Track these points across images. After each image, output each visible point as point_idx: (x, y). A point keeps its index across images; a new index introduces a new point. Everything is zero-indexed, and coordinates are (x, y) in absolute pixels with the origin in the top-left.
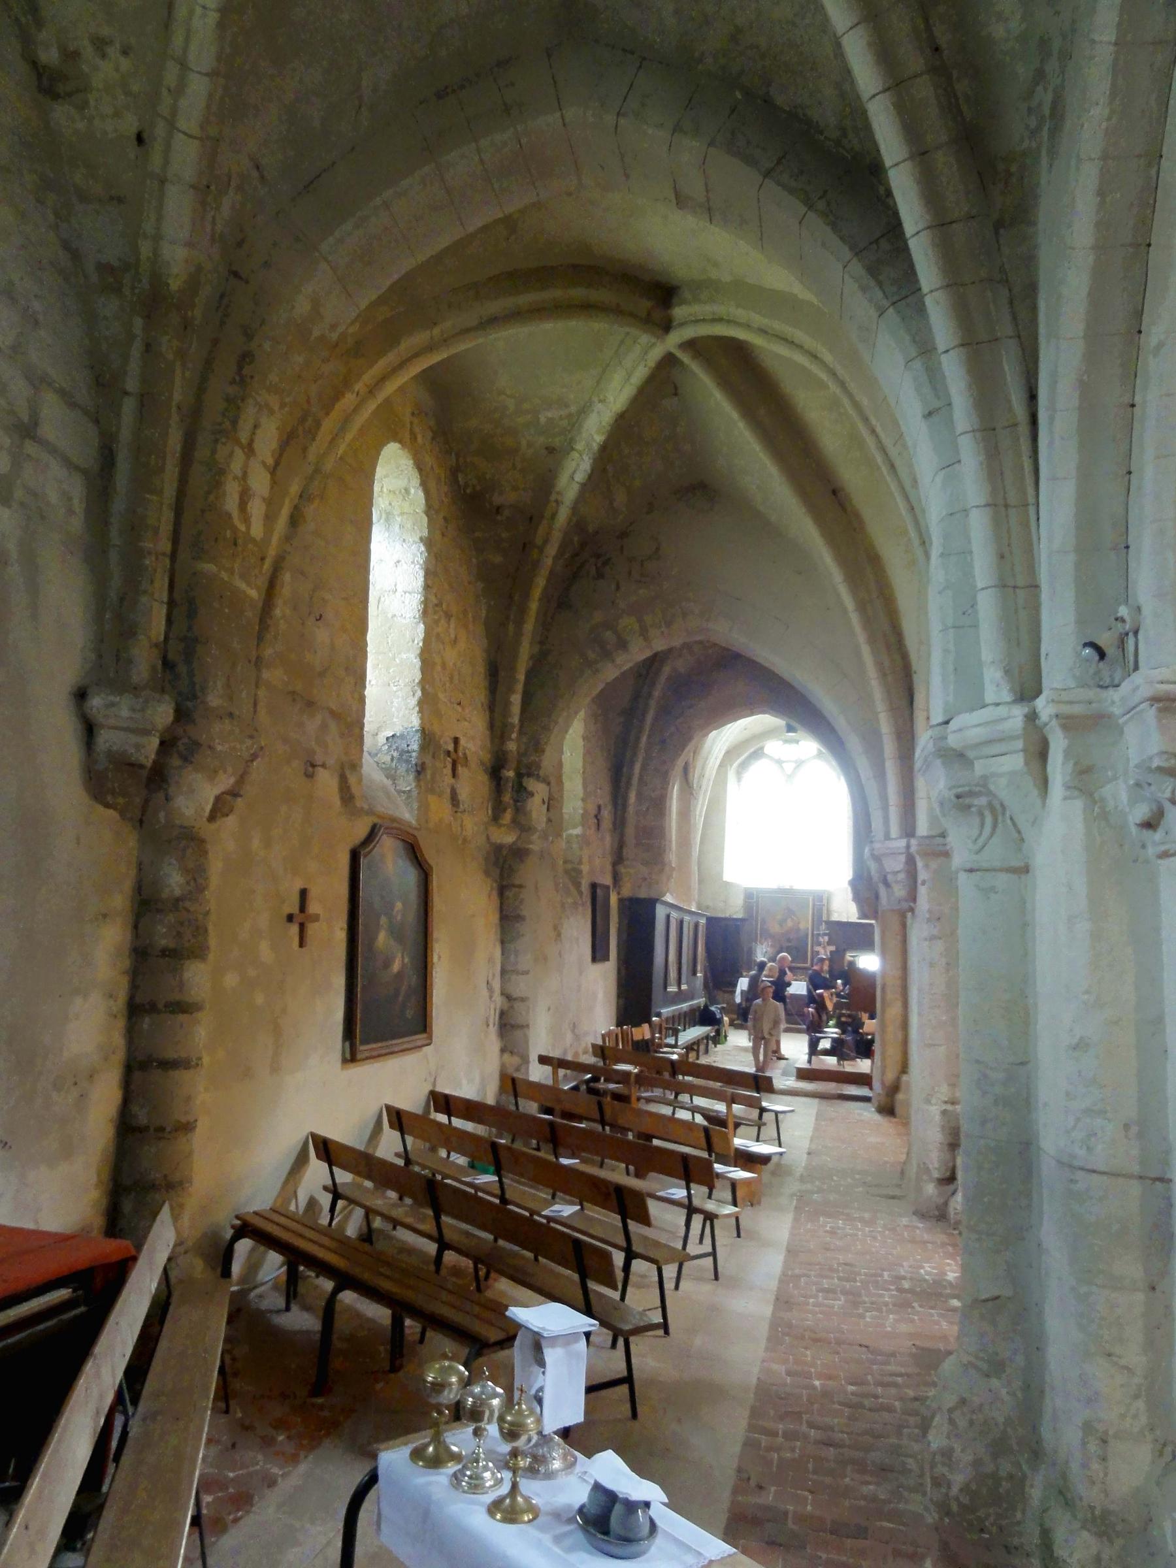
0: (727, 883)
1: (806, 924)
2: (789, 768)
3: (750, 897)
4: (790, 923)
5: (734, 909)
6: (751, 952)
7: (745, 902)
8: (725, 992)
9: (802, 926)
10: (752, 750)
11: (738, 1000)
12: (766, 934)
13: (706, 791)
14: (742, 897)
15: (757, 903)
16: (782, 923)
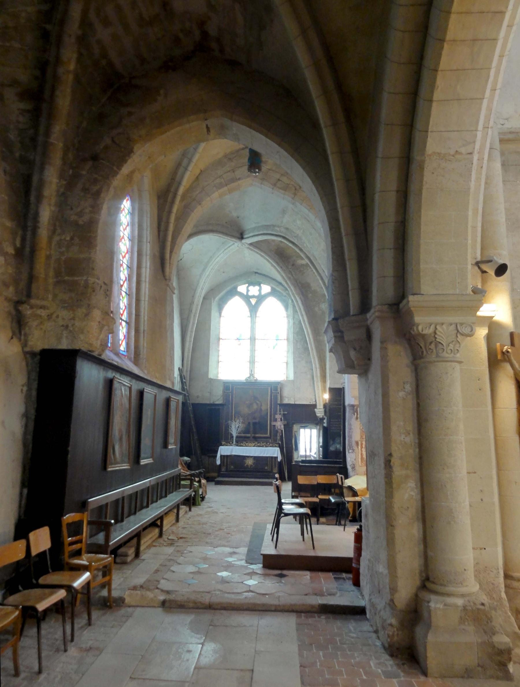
0: (212, 381)
1: (266, 406)
2: (253, 301)
3: (229, 387)
4: (255, 406)
5: (217, 397)
6: (228, 427)
7: (224, 392)
8: (209, 457)
9: (264, 408)
10: (229, 288)
11: (218, 462)
12: (238, 414)
13: (196, 313)
14: (221, 389)
15: (232, 392)
16: (250, 406)
